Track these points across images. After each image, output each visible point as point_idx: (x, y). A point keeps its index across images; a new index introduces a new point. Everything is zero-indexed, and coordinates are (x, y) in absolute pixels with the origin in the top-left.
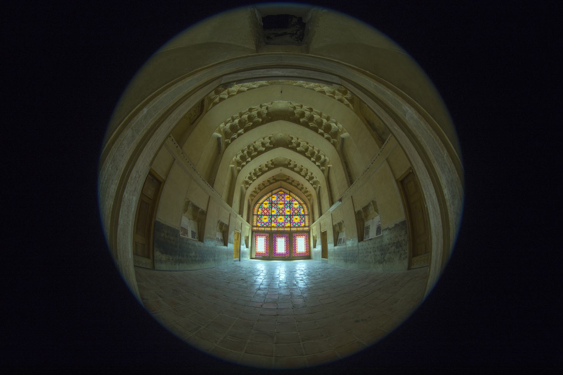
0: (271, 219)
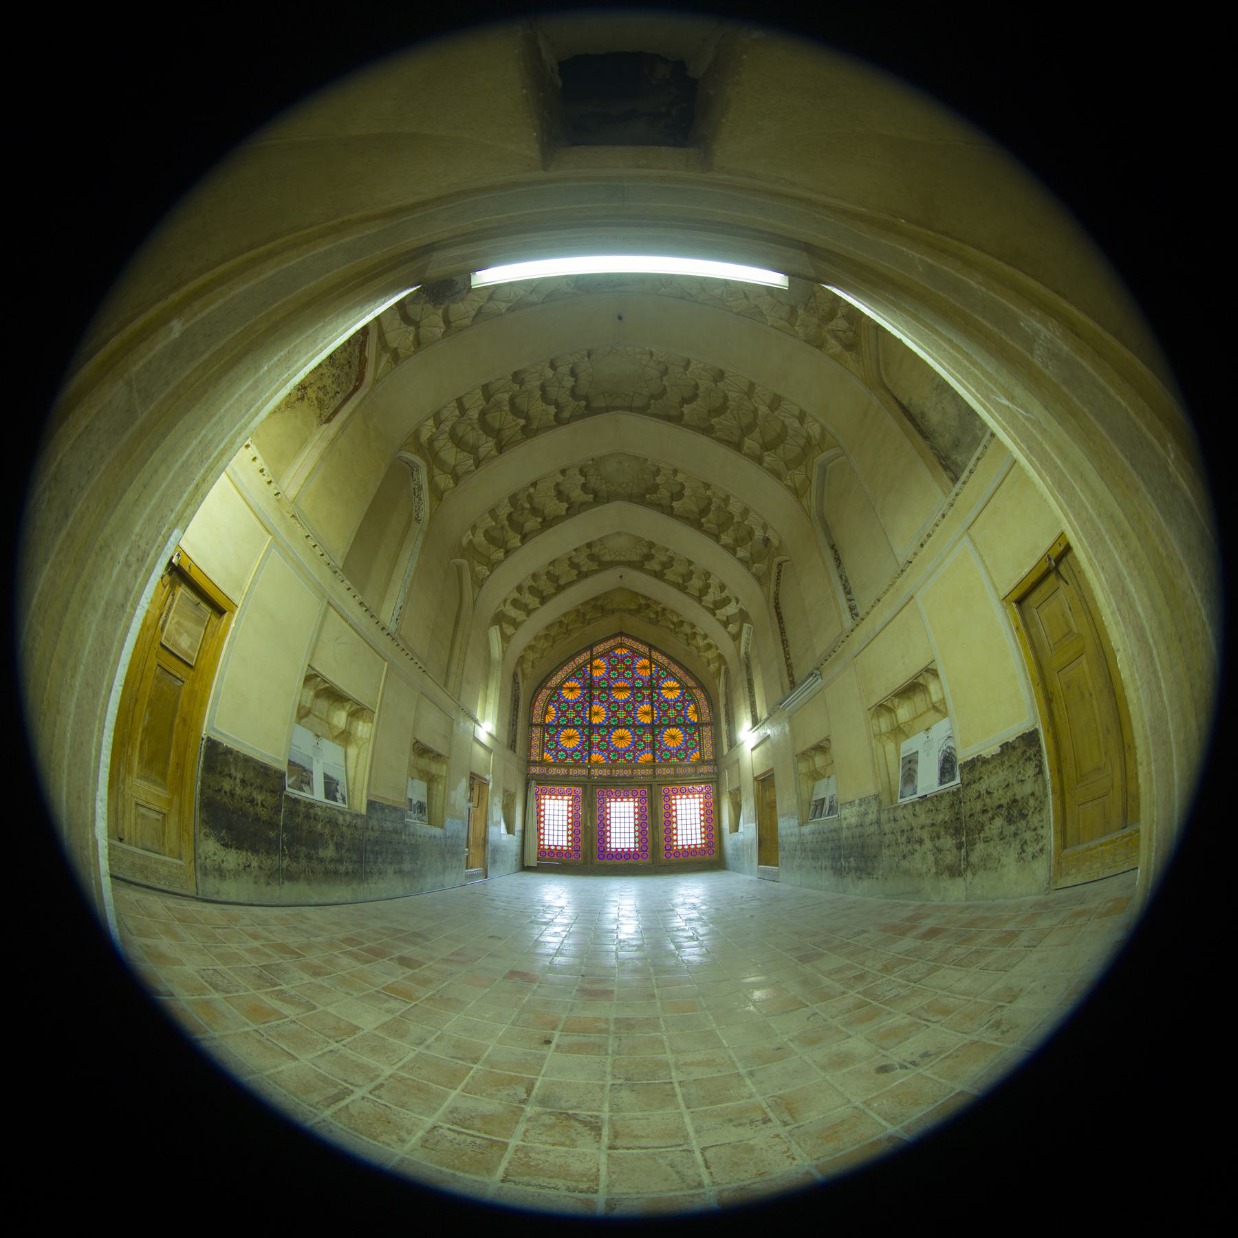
0: (589, 738)
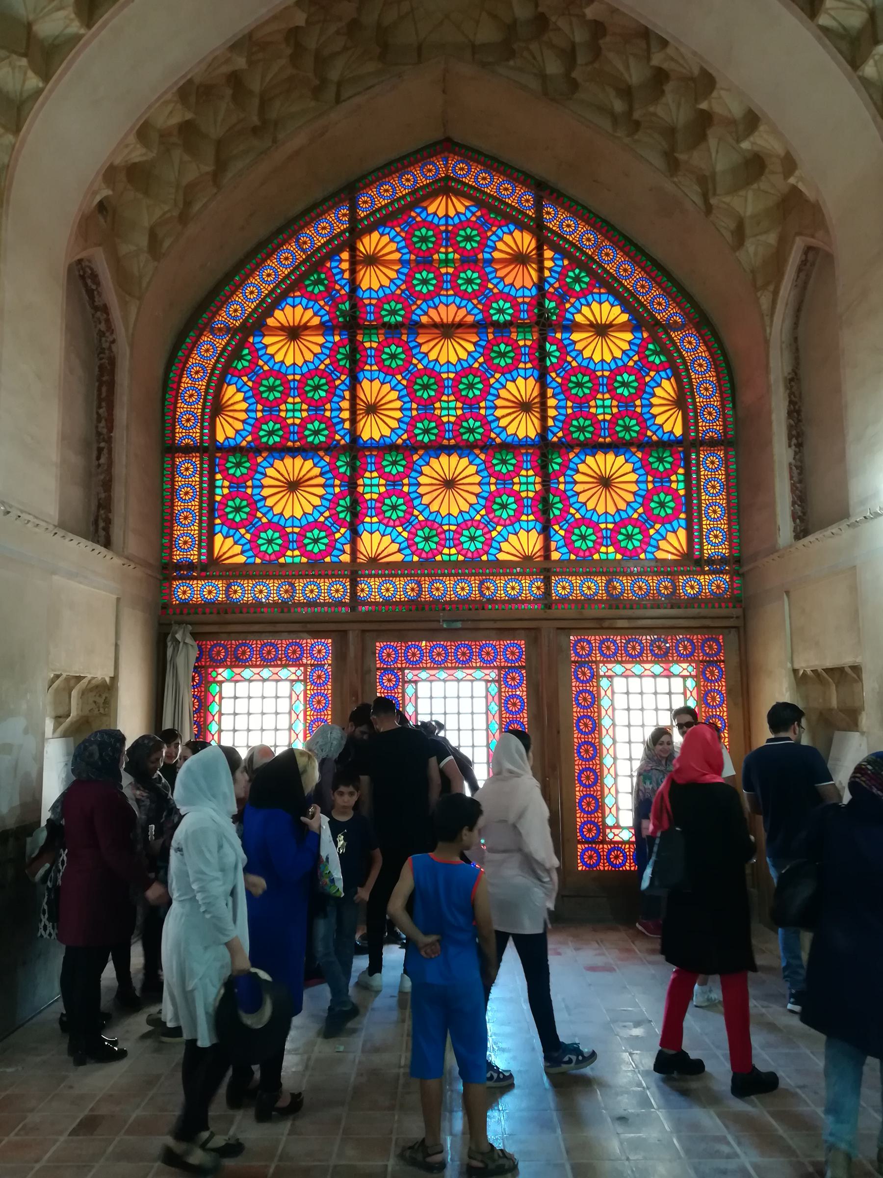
0: (351, 484)
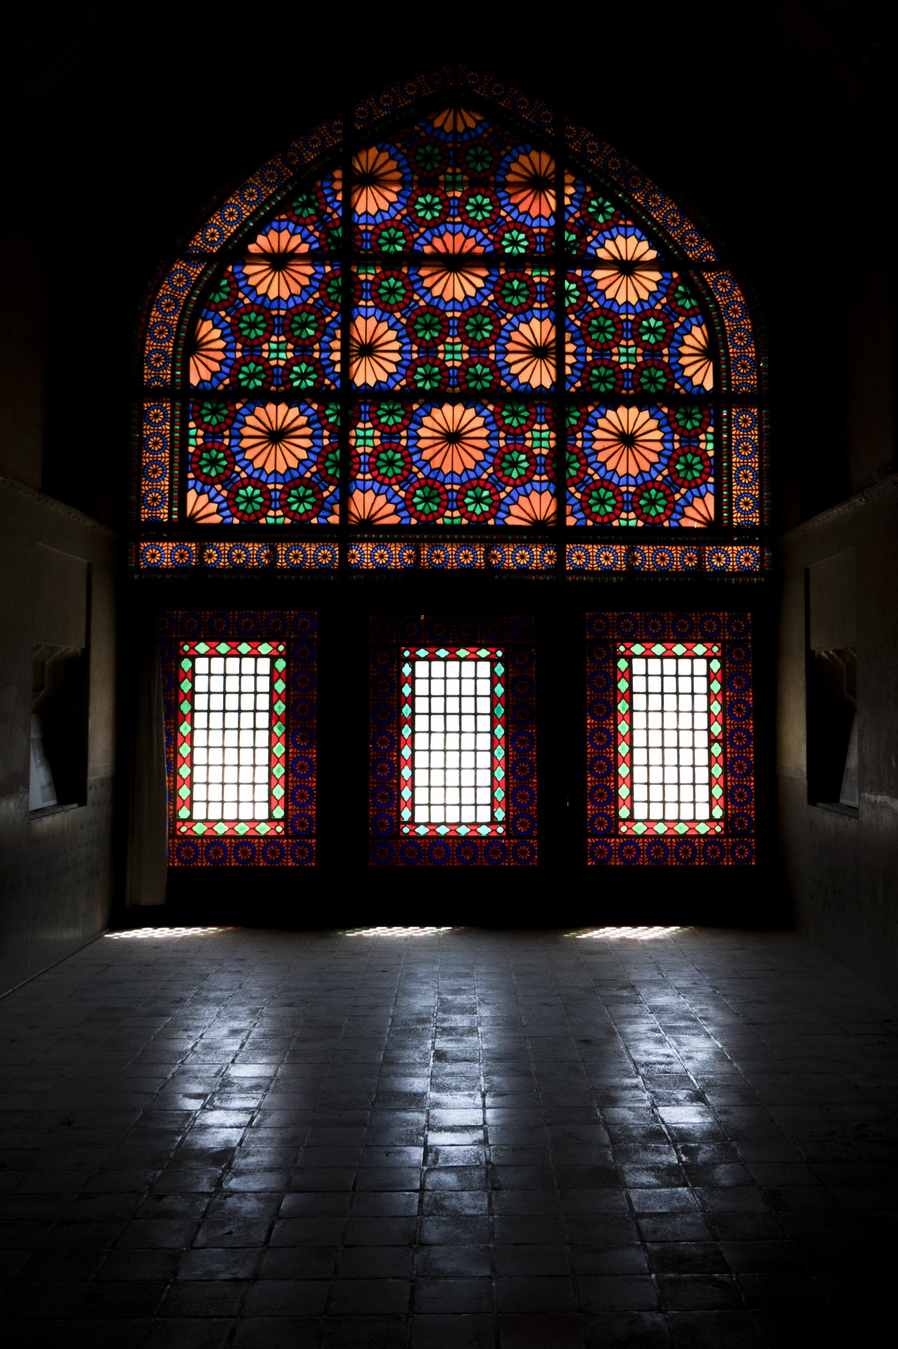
0: (341, 435)
